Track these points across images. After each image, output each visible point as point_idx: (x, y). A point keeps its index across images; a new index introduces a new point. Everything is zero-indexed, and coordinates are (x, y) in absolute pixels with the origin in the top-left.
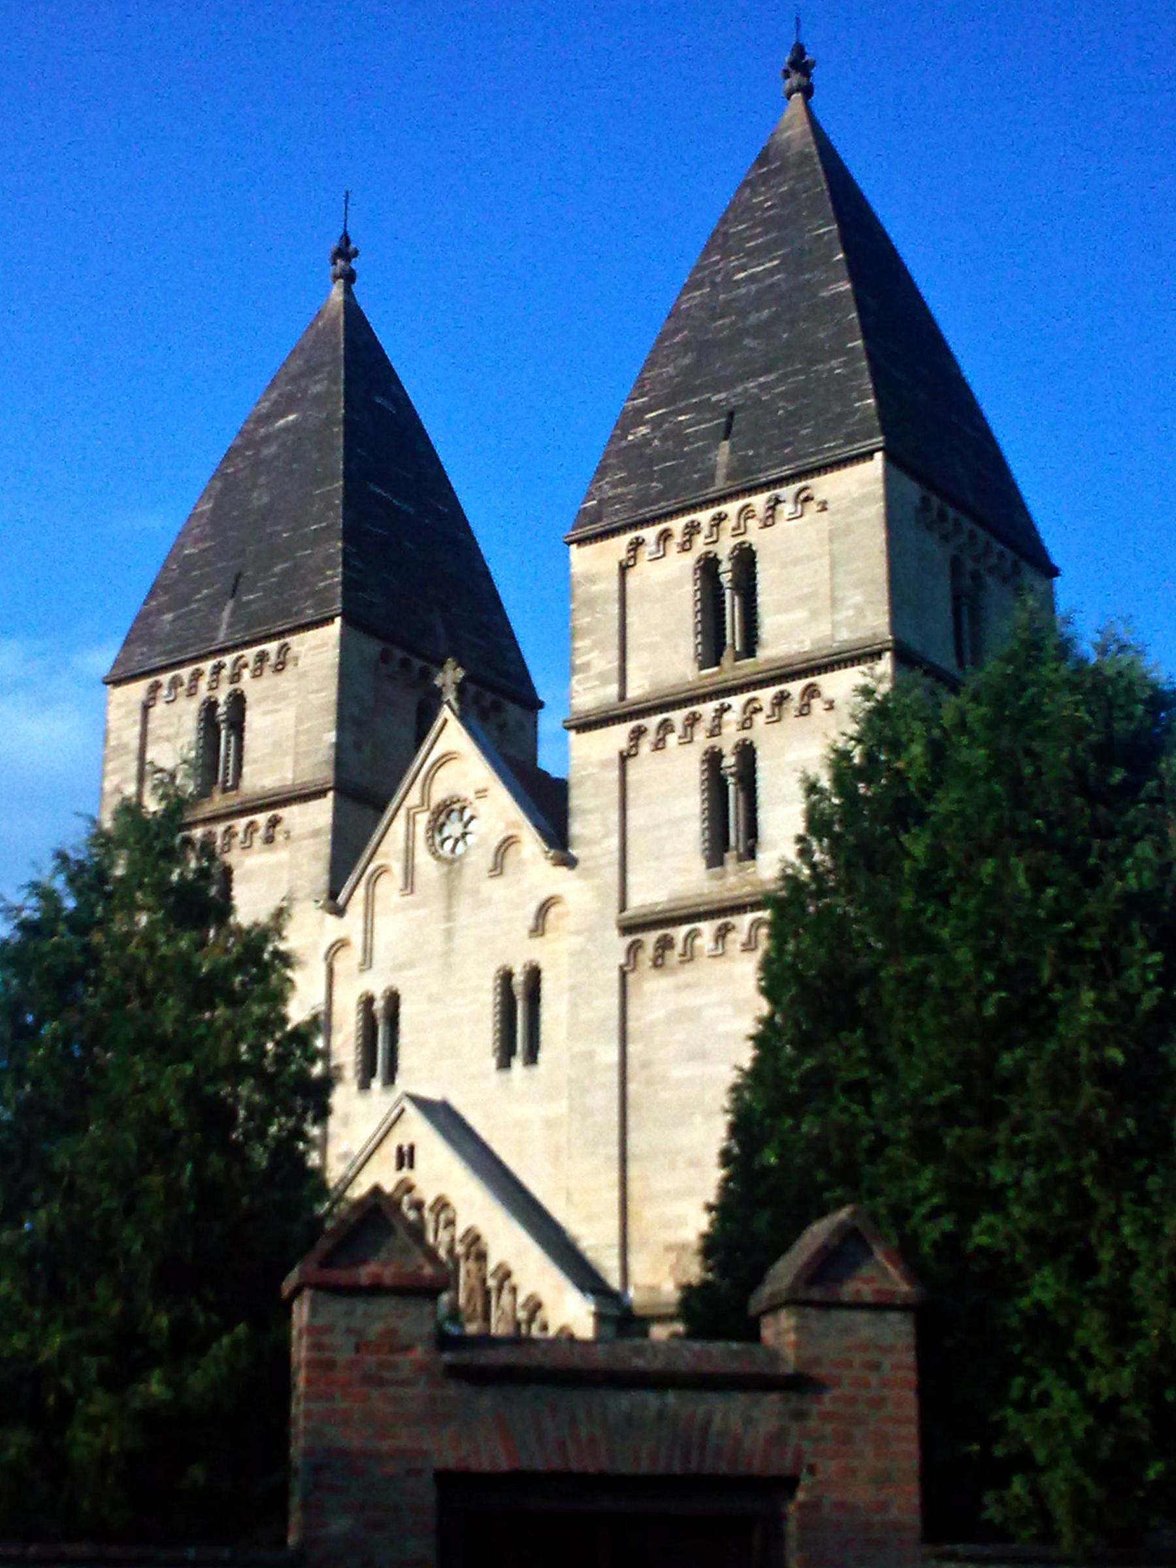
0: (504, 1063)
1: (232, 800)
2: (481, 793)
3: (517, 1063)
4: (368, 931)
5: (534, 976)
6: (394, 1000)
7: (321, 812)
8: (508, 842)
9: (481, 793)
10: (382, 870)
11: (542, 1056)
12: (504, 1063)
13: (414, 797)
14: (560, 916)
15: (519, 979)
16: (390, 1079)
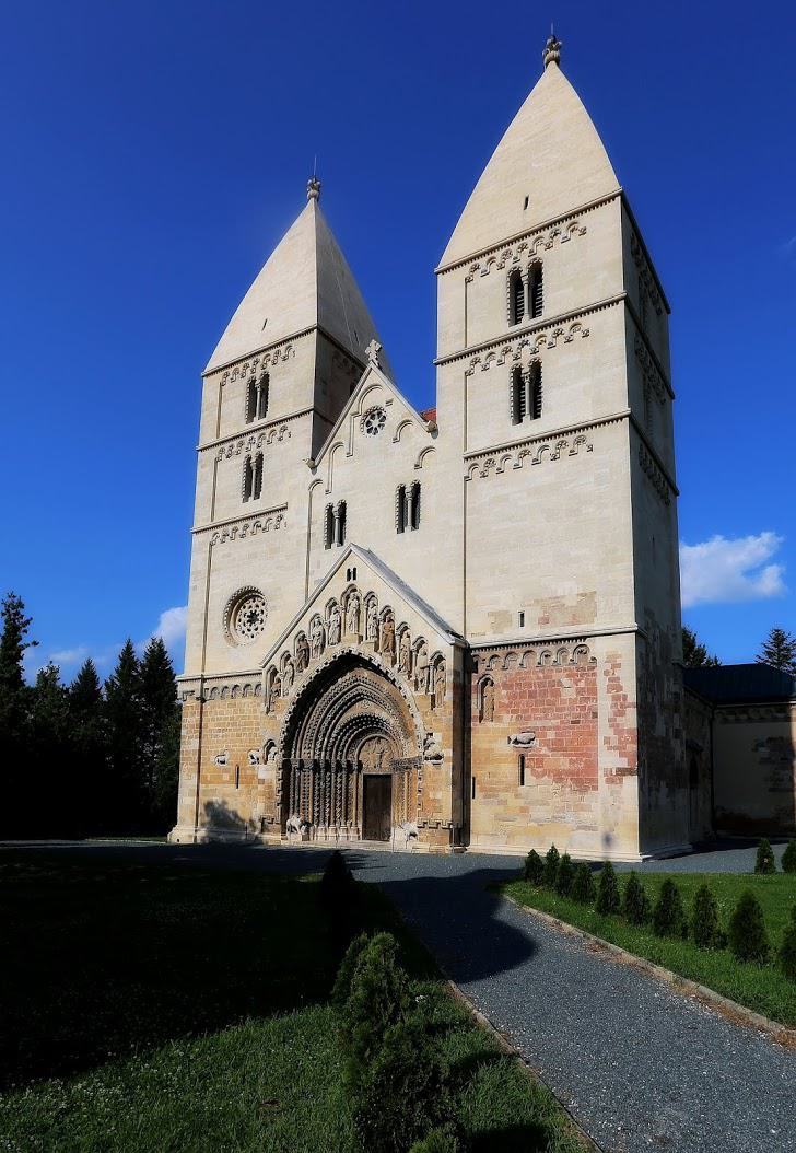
0: (401, 529)
1: (264, 421)
2: (389, 403)
3: (408, 528)
4: (331, 474)
5: (417, 488)
6: (343, 506)
7: (308, 420)
8: (405, 423)
9: (389, 403)
10: (339, 445)
11: (422, 525)
12: (401, 529)
13: (354, 409)
14: (431, 456)
15: (408, 489)
16: (341, 542)
